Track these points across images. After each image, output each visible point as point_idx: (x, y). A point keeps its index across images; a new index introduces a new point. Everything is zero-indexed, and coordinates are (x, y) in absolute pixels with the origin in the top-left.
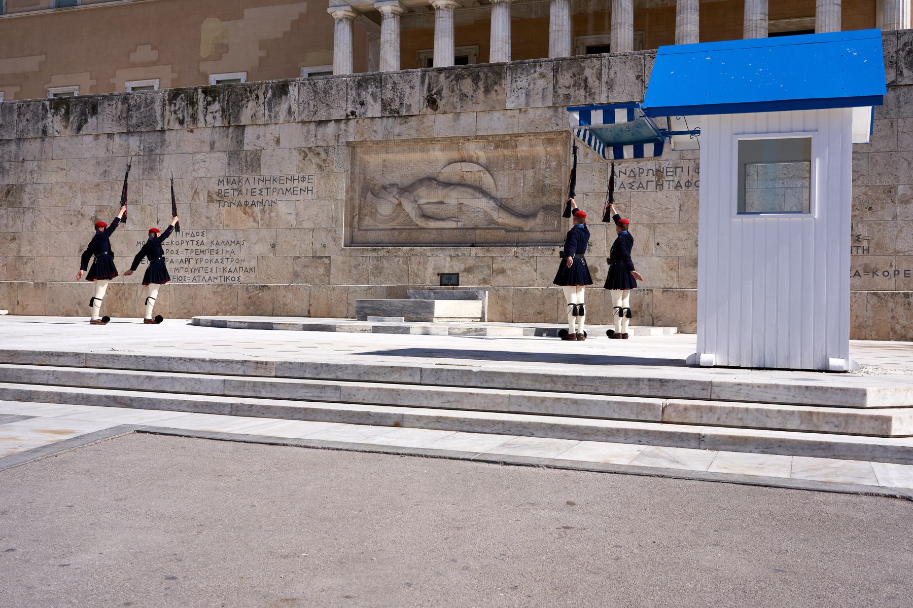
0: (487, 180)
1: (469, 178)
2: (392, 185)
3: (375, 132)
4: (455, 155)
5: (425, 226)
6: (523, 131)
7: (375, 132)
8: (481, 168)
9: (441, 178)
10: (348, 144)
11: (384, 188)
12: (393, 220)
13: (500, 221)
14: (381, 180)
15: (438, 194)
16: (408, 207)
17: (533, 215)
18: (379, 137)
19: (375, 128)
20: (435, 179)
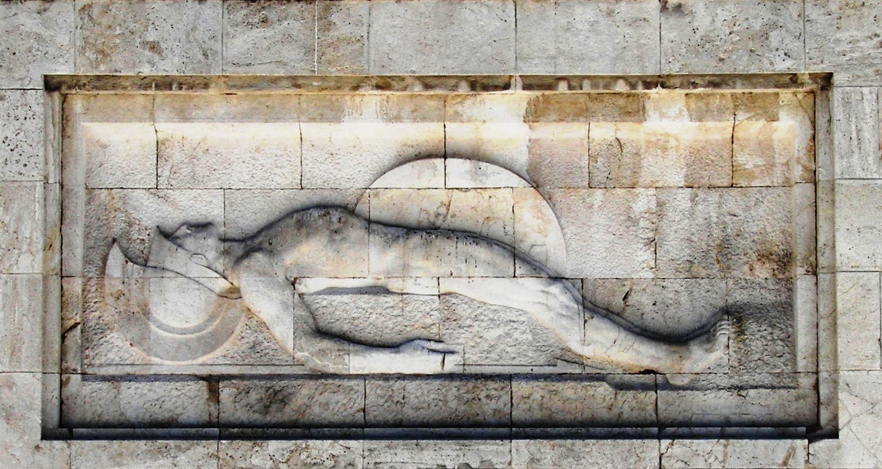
0: (534, 223)
1: (466, 209)
2: (201, 227)
3: (154, 47)
4: (426, 133)
5: (331, 368)
6: (674, 69)
7: (154, 47)
8: (515, 180)
9: (378, 208)
10: (51, 85)
11: (167, 235)
12: (211, 342)
13: (586, 351)
14: (150, 212)
15: (375, 260)
16: (266, 302)
17: (702, 333)
18: (169, 67)
19: (151, 37)
20: (349, 210)
